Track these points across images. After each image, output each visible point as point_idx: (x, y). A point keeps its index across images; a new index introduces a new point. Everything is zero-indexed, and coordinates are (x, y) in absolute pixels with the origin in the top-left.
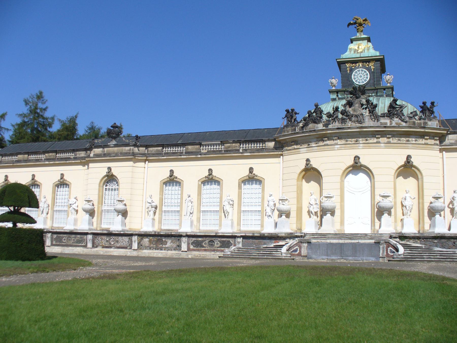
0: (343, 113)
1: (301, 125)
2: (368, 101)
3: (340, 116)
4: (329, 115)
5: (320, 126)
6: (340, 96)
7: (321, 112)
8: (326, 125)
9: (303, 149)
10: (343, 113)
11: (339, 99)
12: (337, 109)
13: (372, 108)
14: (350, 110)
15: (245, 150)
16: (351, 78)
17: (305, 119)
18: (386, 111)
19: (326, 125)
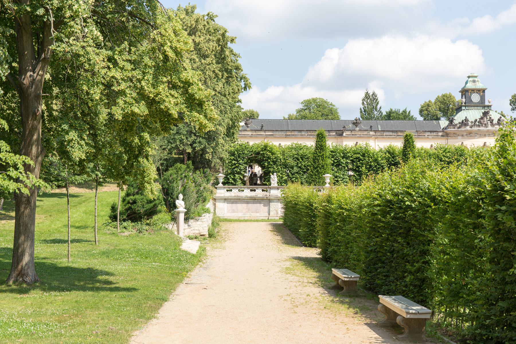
0: (478, 122)
1: (458, 126)
2: (490, 118)
3: (477, 123)
4: (472, 122)
5: (468, 128)
6: (467, 108)
7: (468, 121)
8: (471, 127)
9: (460, 137)
10: (479, 122)
11: (467, 110)
12: (476, 120)
13: (492, 121)
14: (482, 121)
15: (428, 136)
16: (471, 98)
17: (460, 123)
18: (497, 122)
19: (471, 127)
